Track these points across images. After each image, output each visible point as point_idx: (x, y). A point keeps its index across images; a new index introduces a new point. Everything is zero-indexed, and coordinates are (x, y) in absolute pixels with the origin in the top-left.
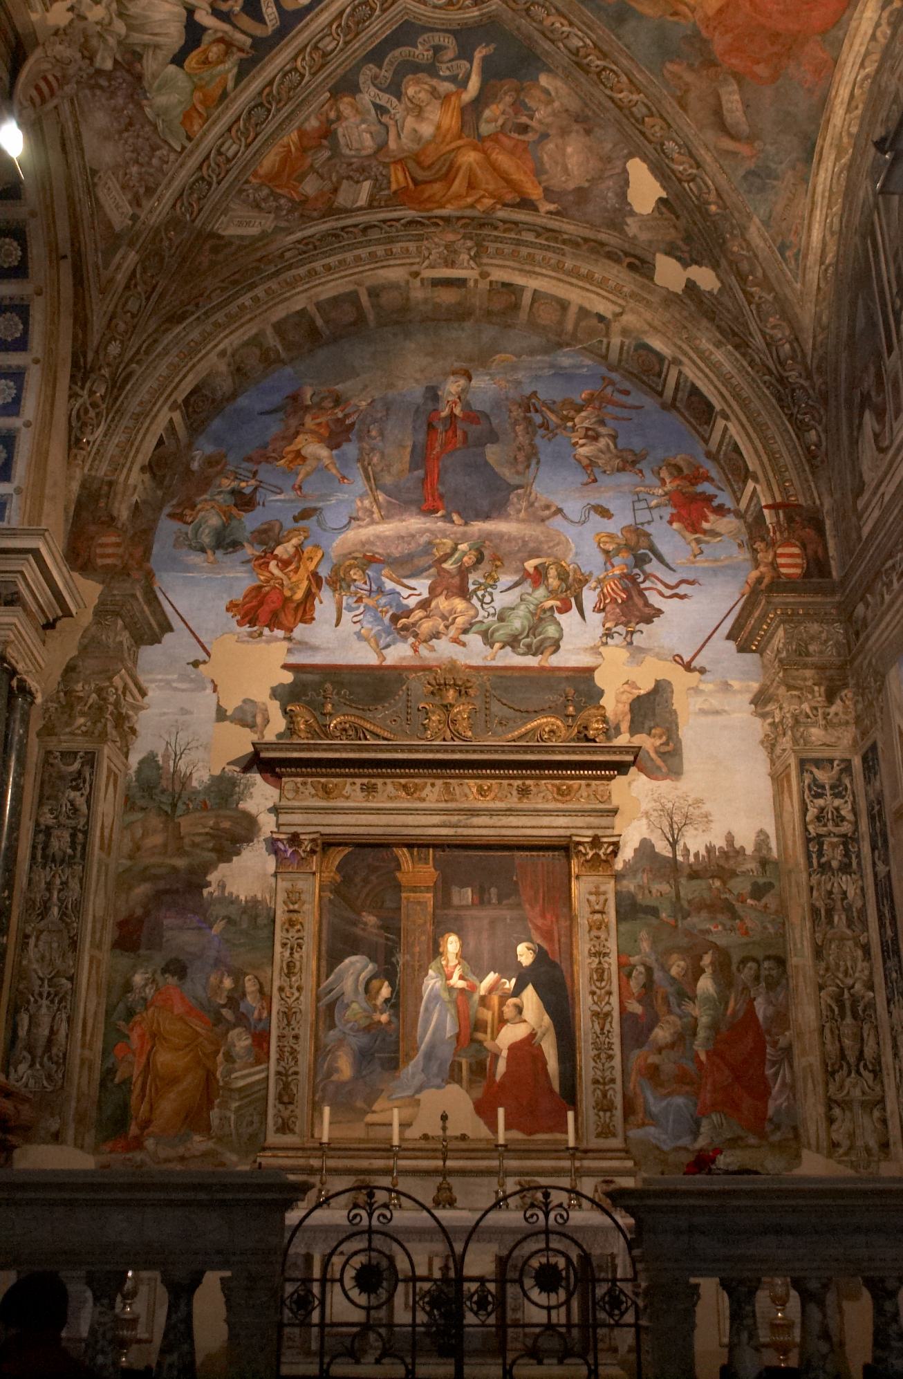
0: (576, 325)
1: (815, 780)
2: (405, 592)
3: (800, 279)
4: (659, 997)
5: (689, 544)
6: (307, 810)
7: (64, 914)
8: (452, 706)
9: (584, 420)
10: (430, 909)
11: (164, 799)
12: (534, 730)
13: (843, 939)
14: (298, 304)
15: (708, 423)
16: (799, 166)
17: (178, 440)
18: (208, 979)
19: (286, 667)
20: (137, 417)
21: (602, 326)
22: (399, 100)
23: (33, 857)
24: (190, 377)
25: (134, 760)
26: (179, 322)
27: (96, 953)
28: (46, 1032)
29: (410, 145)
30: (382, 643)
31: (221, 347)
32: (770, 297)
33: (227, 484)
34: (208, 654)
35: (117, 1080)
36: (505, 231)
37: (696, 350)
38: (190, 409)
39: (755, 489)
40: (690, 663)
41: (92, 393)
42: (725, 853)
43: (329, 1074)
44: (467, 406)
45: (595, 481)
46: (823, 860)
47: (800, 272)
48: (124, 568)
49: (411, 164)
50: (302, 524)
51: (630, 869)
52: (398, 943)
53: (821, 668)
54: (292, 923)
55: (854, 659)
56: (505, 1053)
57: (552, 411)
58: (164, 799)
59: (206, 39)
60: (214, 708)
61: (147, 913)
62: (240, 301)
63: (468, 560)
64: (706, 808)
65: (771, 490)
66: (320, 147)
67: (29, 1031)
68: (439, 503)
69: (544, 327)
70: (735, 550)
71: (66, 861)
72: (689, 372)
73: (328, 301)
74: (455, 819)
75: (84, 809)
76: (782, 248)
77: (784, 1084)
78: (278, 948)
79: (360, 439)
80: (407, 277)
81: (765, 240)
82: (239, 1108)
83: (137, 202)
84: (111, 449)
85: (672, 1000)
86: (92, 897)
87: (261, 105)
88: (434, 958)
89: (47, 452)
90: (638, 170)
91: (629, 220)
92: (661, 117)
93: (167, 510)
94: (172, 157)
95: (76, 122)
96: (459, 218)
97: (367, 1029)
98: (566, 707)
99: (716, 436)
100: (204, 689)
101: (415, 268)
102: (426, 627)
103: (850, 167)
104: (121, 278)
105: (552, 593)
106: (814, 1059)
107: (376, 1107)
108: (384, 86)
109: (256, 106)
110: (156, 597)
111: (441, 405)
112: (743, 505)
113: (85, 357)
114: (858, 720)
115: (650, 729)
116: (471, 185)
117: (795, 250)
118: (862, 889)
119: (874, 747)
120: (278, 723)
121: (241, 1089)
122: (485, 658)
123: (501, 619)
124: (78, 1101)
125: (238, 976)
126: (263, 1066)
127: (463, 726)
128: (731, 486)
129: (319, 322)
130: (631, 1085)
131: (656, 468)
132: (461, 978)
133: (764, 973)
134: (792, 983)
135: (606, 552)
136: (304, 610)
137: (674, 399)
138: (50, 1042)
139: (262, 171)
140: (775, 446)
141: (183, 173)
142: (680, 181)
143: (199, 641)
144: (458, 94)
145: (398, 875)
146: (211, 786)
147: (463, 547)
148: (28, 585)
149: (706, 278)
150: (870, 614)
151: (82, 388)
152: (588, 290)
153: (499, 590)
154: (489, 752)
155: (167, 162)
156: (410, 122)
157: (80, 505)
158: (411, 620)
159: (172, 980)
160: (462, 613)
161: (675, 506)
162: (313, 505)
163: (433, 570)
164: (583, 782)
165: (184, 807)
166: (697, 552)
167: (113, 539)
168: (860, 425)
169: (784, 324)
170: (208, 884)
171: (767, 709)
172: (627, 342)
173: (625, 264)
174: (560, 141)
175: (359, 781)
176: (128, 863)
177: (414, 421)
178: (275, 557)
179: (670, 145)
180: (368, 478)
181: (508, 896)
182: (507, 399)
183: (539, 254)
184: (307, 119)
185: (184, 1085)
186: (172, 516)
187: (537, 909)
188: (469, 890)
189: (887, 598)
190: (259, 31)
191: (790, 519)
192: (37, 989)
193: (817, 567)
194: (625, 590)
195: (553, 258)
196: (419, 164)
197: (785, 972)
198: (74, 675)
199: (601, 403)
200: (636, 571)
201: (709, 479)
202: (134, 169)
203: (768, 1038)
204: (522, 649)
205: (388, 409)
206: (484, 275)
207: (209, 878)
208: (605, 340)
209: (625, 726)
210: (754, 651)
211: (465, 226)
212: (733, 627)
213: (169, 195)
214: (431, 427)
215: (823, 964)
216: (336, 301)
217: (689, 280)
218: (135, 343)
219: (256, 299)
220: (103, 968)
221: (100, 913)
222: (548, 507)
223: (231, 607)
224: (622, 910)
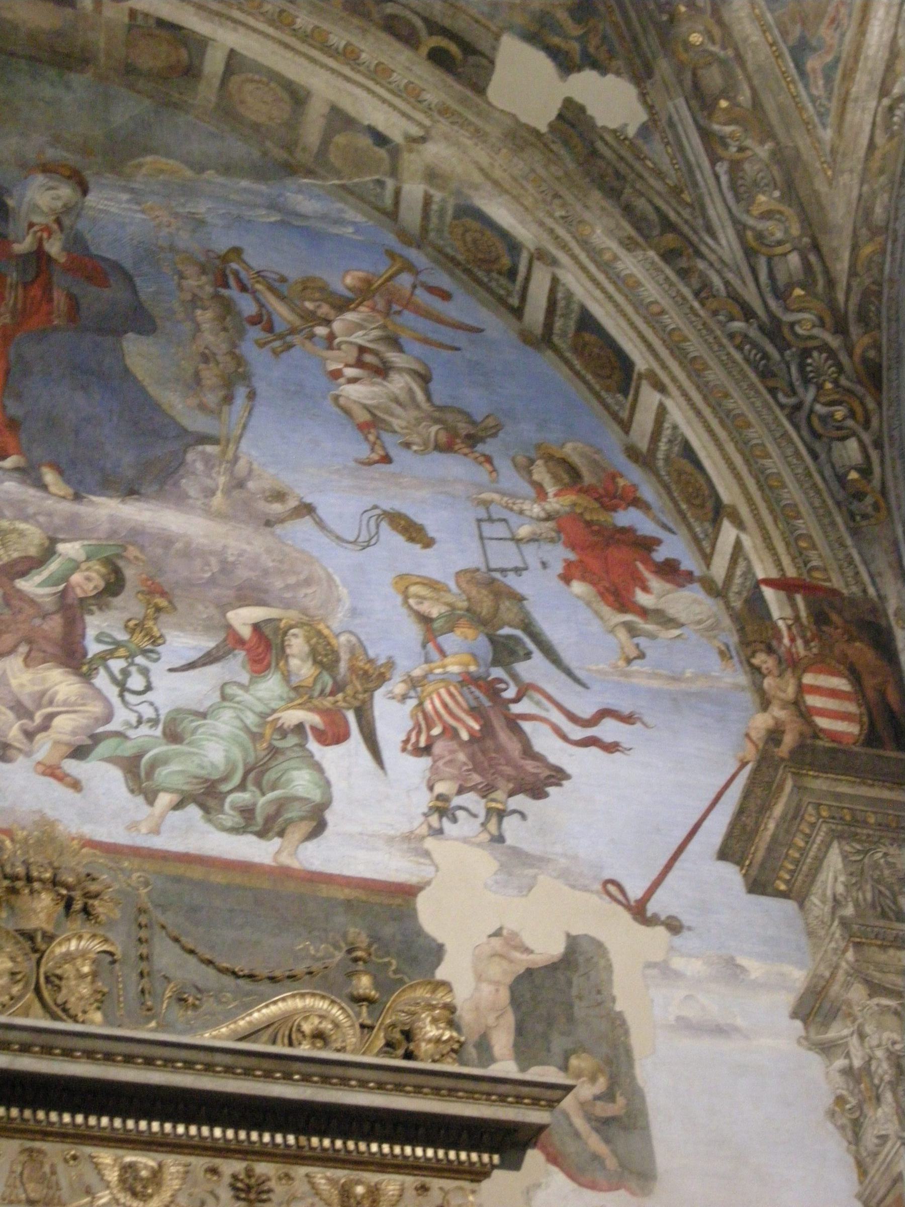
0: (326, 141)
3: (831, 119)
5: (612, 631)
8: (49, 938)
15: (625, 392)
21: (382, 153)
32: (763, 151)
37: (584, 243)
39: (738, 546)
45: (386, 459)
47: (834, 105)
57: (282, 298)
65: (771, 548)
69: (256, 127)
70: (714, 663)
81: (765, 29)
98: (350, 975)
99: (644, 420)
112: (719, 568)
115: (567, 1055)
117: (829, 58)
122: (133, 826)
123: (173, 736)
128: (690, 528)
131: (520, 459)
135: (425, 620)
140: (767, 462)
147: (70, 549)
152: (347, 79)
154: (169, 1063)
160: (70, 708)
161: (572, 545)
164: (410, 1181)
166: (633, 653)
169: (788, 211)
172: (437, 195)
173: (424, 51)
182: (172, 248)
191: (820, 618)
194: (475, 711)
199: (389, 303)
200: (497, 672)
201: (636, 502)
210: (784, 895)
212: (729, 835)
217: (568, 103)
222: (279, 496)
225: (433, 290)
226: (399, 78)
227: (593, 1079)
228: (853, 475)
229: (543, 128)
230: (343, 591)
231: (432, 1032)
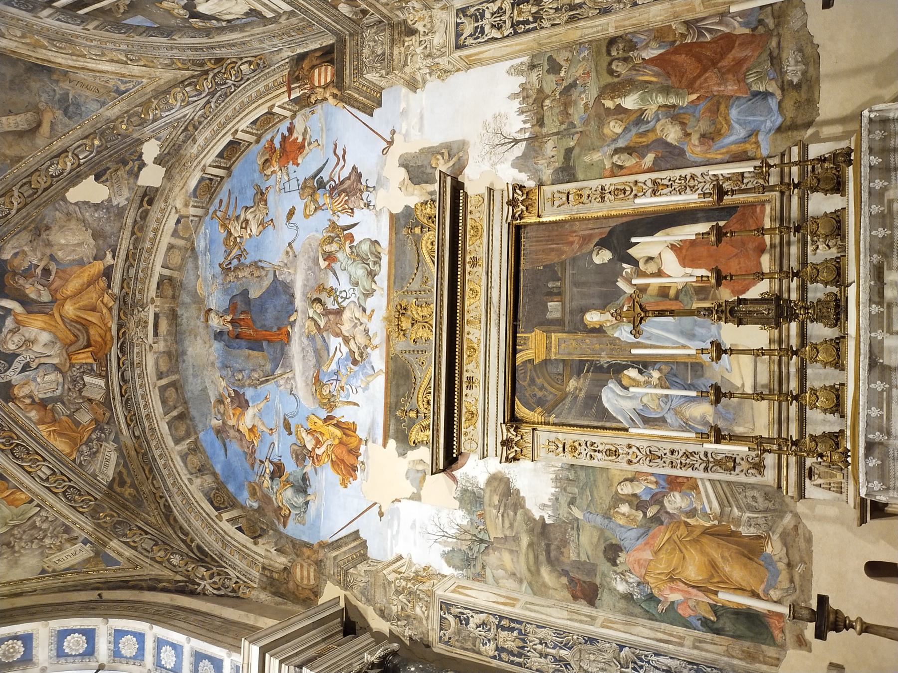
0: (183, 238)
1: (471, 35)
2: (338, 354)
4: (641, 140)
7: (565, 645)
10: (564, 335)
11: (476, 549)
14: (164, 428)
17: (240, 517)
18: (621, 526)
19: (385, 445)
20: (225, 545)
21: (182, 221)
22: (18, 355)
24: (203, 505)
25: (448, 571)
26: (172, 511)
27: (599, 621)
29: (56, 349)
30: (371, 372)
31: (186, 482)
33: (267, 483)
34: (375, 504)
35: (713, 618)
37: (197, 156)
38: (222, 506)
40: (387, 142)
41: (203, 578)
42: (524, 99)
44: (226, 312)
45: (272, 220)
46: (531, 19)
47: (135, 80)
48: (316, 564)
49: (72, 349)
50: (293, 429)
51: (534, 173)
58: (476, 549)
60: (411, 501)
61: (565, 573)
63: (319, 308)
64: (490, 119)
65: (279, 95)
68: (284, 330)
71: (523, 636)
73: (163, 408)
74: (494, 316)
75: (483, 616)
77: (720, 23)
78: (594, 463)
79: (243, 386)
80: (152, 353)
82: (740, 508)
83: (73, 540)
84: (242, 565)
85: (643, 128)
86: (552, 619)
87: (12, 451)
88: (605, 332)
91: (115, 203)
93: (281, 527)
94: (43, 513)
96: (119, 318)
99: (247, 137)
100: (398, 509)
102: (361, 339)
104: (128, 553)
107: (738, 384)
108: (7, 365)
109: (13, 454)
112: (288, 114)
113: (179, 581)
116: (93, 309)
121: (721, 505)
122: (382, 295)
123: (357, 284)
124: (733, 657)
125: (618, 499)
126: (700, 483)
129: (175, 413)
130: (719, 157)
131: (265, 178)
136: (347, 429)
137: (224, 168)
139: (67, 450)
142: (79, 165)
143: (366, 510)
144: (16, 315)
146: (467, 510)
147: (311, 313)
148: (297, 654)
151: (199, 585)
153: (338, 286)
155: (47, 517)
157: (275, 594)
158: (356, 350)
159: (622, 558)
162: (282, 420)
163: (325, 334)
164: (469, 216)
165: (482, 533)
167: (298, 570)
171: (420, 79)
172: (192, 203)
175: (465, 391)
176: (525, 584)
178: (314, 449)
180: (267, 381)
181: (555, 272)
184: (29, 419)
185: (716, 555)
186: (285, 526)
187: (566, 249)
188: (549, 304)
191: (297, 79)
194: (339, 195)
195: (145, 255)
197: (621, 37)
198: (386, 611)
201: (272, 140)
202: (47, 541)
203: (678, 43)
204: (376, 268)
207: (537, 518)
208: (191, 218)
211: (125, 314)
212: (365, 113)
213: (73, 516)
214: (238, 337)
216: (164, 402)
217: (154, 163)
219: (161, 456)
220: (611, 617)
221: (565, 614)
222: (287, 253)
224: (567, 178)
225: (220, 206)
226: (159, 215)
227: (438, 159)
228: (252, 67)
230: (311, 234)
231: (428, 210)
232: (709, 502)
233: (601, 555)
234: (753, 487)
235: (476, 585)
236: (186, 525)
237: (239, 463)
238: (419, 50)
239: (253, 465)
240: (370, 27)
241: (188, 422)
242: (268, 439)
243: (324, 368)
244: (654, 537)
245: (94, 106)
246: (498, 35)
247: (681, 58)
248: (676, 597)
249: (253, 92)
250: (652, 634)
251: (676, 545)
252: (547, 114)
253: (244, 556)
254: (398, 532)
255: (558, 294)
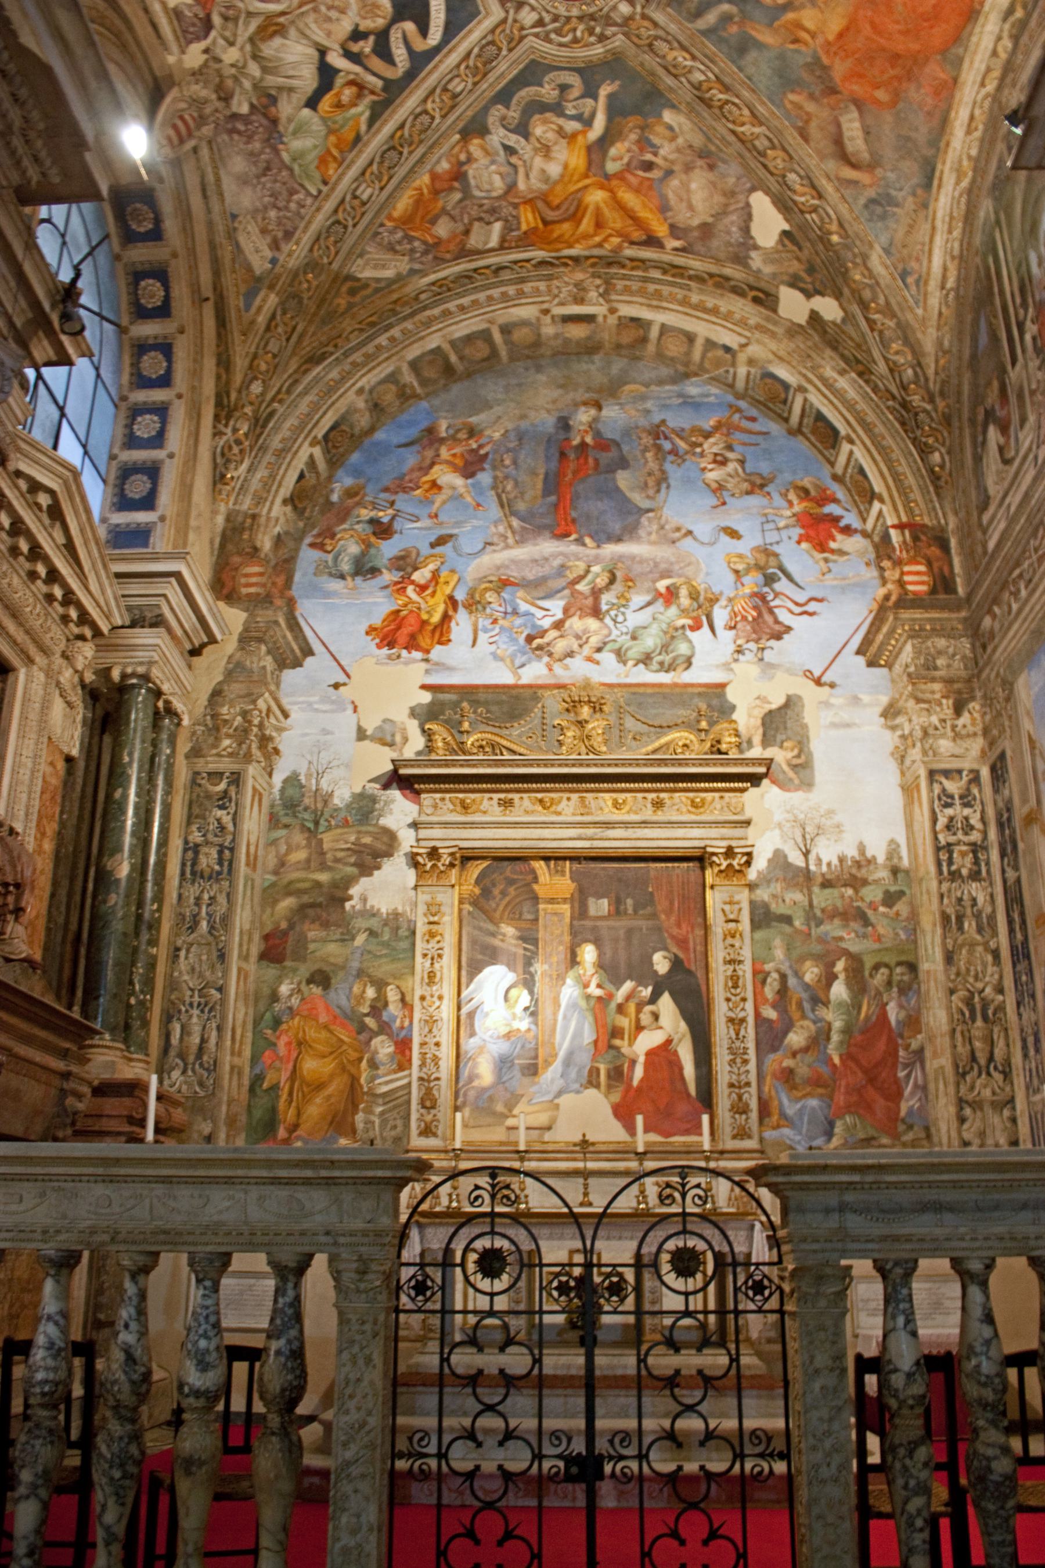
0: (703, 356)
1: (944, 790)
2: (540, 613)
6: (446, 825)
9: (712, 446)
10: (568, 920)
11: (306, 816)
12: (667, 745)
13: (972, 945)
14: (433, 342)
16: (919, 192)
17: (317, 473)
19: (424, 687)
21: (728, 356)
23: (183, 874)
25: (278, 779)
27: (244, 965)
28: (197, 1041)
30: (518, 663)
32: (891, 324)
33: (365, 514)
34: (348, 676)
35: (265, 1086)
36: (633, 269)
39: (880, 513)
41: (235, 430)
43: (471, 1079)
44: (598, 434)
45: (724, 503)
46: (954, 868)
49: (540, 204)
50: (439, 550)
51: (765, 879)
52: (536, 953)
53: (948, 681)
54: (432, 935)
55: (980, 672)
56: (642, 1059)
57: (682, 438)
58: (306, 816)
59: (339, 81)
61: (292, 926)
62: (377, 342)
63: (602, 581)
64: (838, 818)
66: (451, 189)
67: (181, 1039)
69: (672, 359)
70: (863, 568)
71: (215, 877)
72: (816, 400)
73: (460, 339)
74: (590, 832)
75: (230, 827)
76: (904, 275)
77: (916, 1086)
78: (419, 958)
79: (494, 468)
82: (382, 1113)
83: (275, 246)
84: (255, 484)
85: (807, 1006)
87: (393, 148)
89: (191, 486)
90: (761, 203)
91: (753, 254)
92: (784, 150)
93: (308, 540)
94: (309, 201)
95: (216, 168)
96: (587, 258)
97: (508, 1036)
99: (842, 459)
101: (545, 306)
102: (560, 647)
103: (970, 191)
104: (262, 320)
105: (684, 612)
106: (945, 1061)
107: (515, 1112)
110: (298, 624)
111: (572, 434)
112: (869, 526)
114: (986, 731)
116: (599, 225)
118: (992, 895)
119: (1002, 756)
120: (417, 742)
123: (634, 638)
125: (380, 985)
127: (597, 742)
129: (453, 358)
130: (766, 1089)
132: (599, 986)
133: (896, 978)
134: (923, 988)
135: (737, 572)
136: (441, 632)
137: (801, 423)
138: (201, 1050)
141: (320, 217)
142: (802, 212)
144: (584, 133)
145: (535, 887)
147: (596, 569)
149: (829, 308)
150: (997, 626)
156: (538, 162)
157: (224, 536)
158: (546, 640)
159: (317, 990)
160: (596, 633)
163: (567, 592)
164: (717, 795)
167: (256, 569)
168: (984, 442)
170: (350, 898)
174: (684, 177)
175: (496, 796)
176: (273, 878)
177: (547, 449)
178: (413, 582)
179: (792, 177)
180: (502, 506)
181: (644, 907)
183: (666, 290)
184: (438, 162)
185: (330, 1090)
186: (312, 545)
187: (673, 919)
189: (1015, 607)
190: (391, 73)
191: (916, 539)
192: (188, 1000)
193: (943, 584)
195: (680, 293)
196: (548, 204)
197: (917, 977)
200: (766, 589)
201: (836, 501)
202: (273, 214)
204: (655, 666)
205: (520, 439)
206: (613, 311)
207: (351, 892)
209: (757, 739)
211: (593, 265)
213: (307, 239)
214: (563, 455)
215: (954, 970)
216: (469, 339)
218: (276, 384)
219: (392, 339)
221: (247, 926)
222: (678, 529)
223: (371, 631)
229: (803, 322)
232: (387, 1083)
233: (316, 967)
234: (407, 1125)
235: (265, 818)
236: (300, 388)
237: (389, 468)
238: (934, 720)
239: (386, 490)
240: (973, 646)
241: (442, 382)
242: (423, 512)
243: (521, 593)
244: (343, 1026)
245: (884, 239)
246: (940, 825)
247: (881, 1045)
248: (282, 1049)
249: (904, 468)
250: (239, 1023)
251: (336, 1049)
252: (835, 892)
253: (267, 485)
254: (317, 710)
255: (617, 910)
